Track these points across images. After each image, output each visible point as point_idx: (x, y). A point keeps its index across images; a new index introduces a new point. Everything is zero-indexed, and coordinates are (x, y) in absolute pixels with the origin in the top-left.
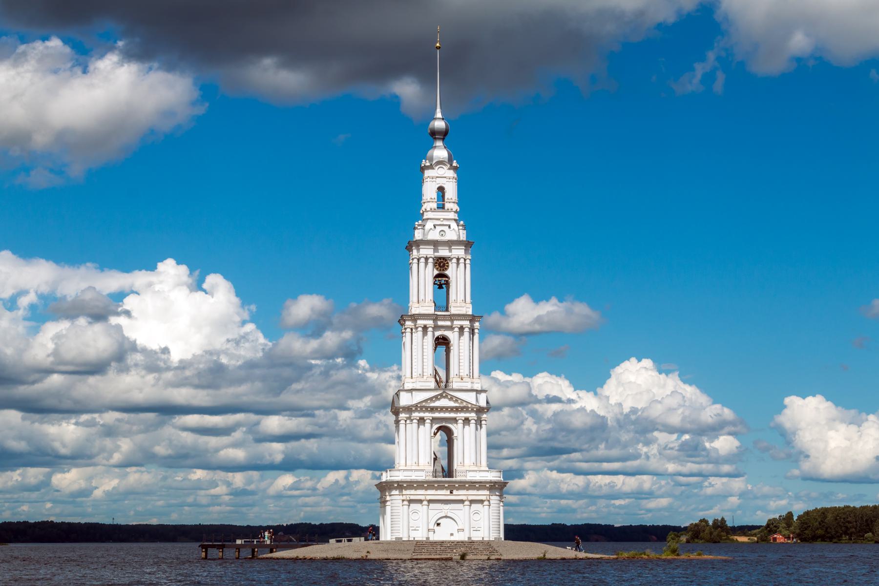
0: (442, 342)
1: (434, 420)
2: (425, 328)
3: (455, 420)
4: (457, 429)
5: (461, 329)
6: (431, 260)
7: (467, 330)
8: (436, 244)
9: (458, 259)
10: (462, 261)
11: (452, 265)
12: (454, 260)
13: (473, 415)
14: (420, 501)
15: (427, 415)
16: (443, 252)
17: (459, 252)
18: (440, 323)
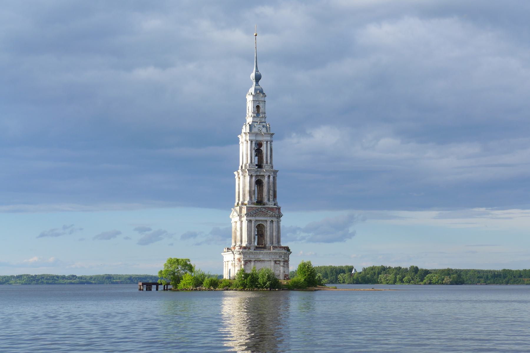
0: (259, 183)
1: (256, 221)
2: (251, 176)
3: (266, 221)
4: (268, 226)
5: (269, 176)
6: (253, 142)
7: (271, 177)
8: (256, 134)
9: (267, 142)
10: (269, 143)
11: (264, 145)
12: (265, 142)
13: (275, 219)
14: (250, 261)
15: (253, 219)
16: (260, 138)
17: (269, 138)
18: (258, 174)
